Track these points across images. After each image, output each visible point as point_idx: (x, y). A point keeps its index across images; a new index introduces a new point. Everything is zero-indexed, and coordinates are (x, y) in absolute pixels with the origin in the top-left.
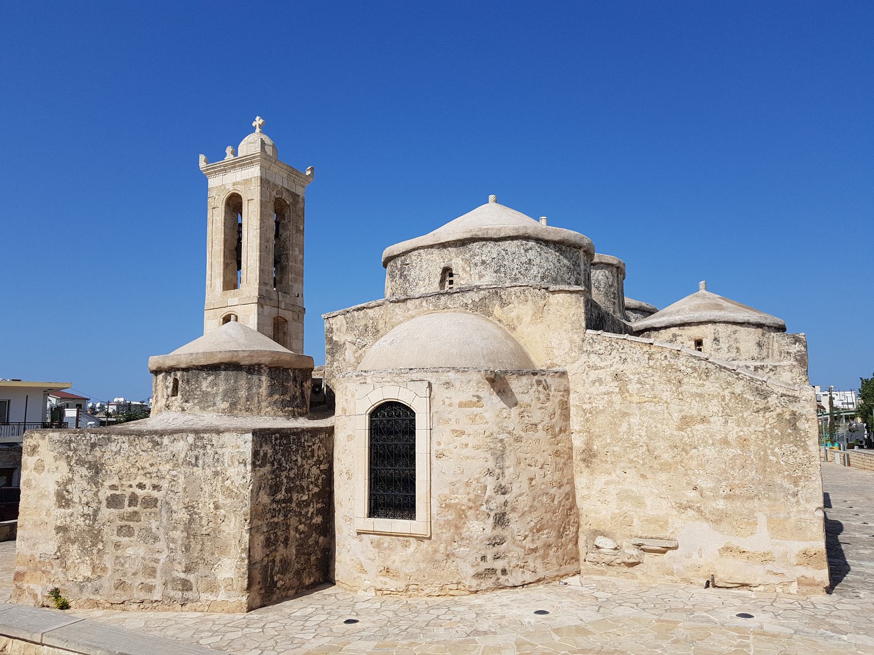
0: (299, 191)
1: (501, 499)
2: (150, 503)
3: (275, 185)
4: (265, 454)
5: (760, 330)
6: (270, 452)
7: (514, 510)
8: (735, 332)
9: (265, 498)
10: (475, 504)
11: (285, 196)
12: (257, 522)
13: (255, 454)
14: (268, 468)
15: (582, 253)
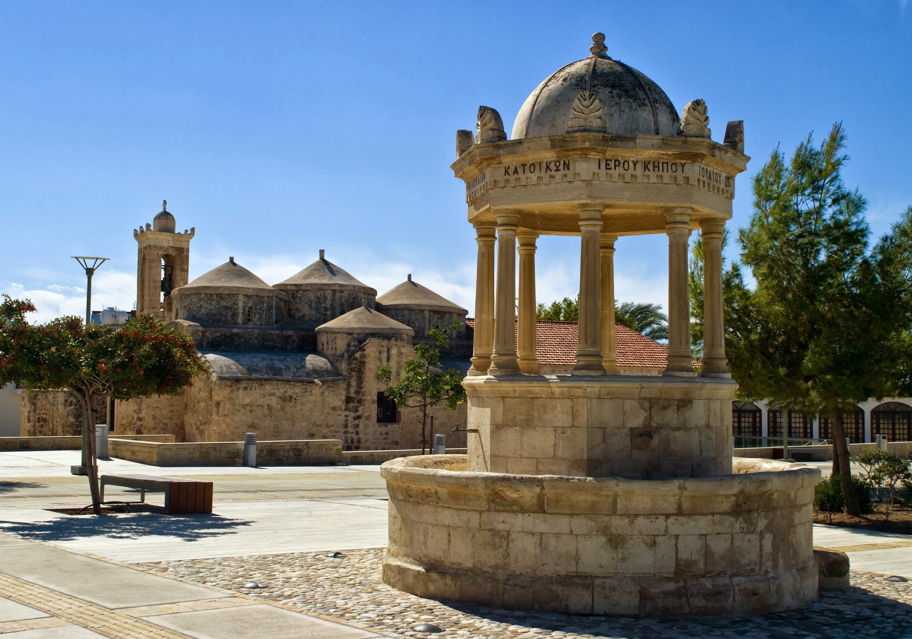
0: (184, 245)
1: (139, 423)
2: (45, 420)
3: (161, 248)
4: (71, 402)
5: (350, 337)
6: (74, 401)
7: (145, 428)
8: (335, 338)
9: (71, 419)
10: (130, 423)
11: (171, 252)
12: (66, 428)
13: (66, 401)
14: (73, 407)
15: (241, 297)
